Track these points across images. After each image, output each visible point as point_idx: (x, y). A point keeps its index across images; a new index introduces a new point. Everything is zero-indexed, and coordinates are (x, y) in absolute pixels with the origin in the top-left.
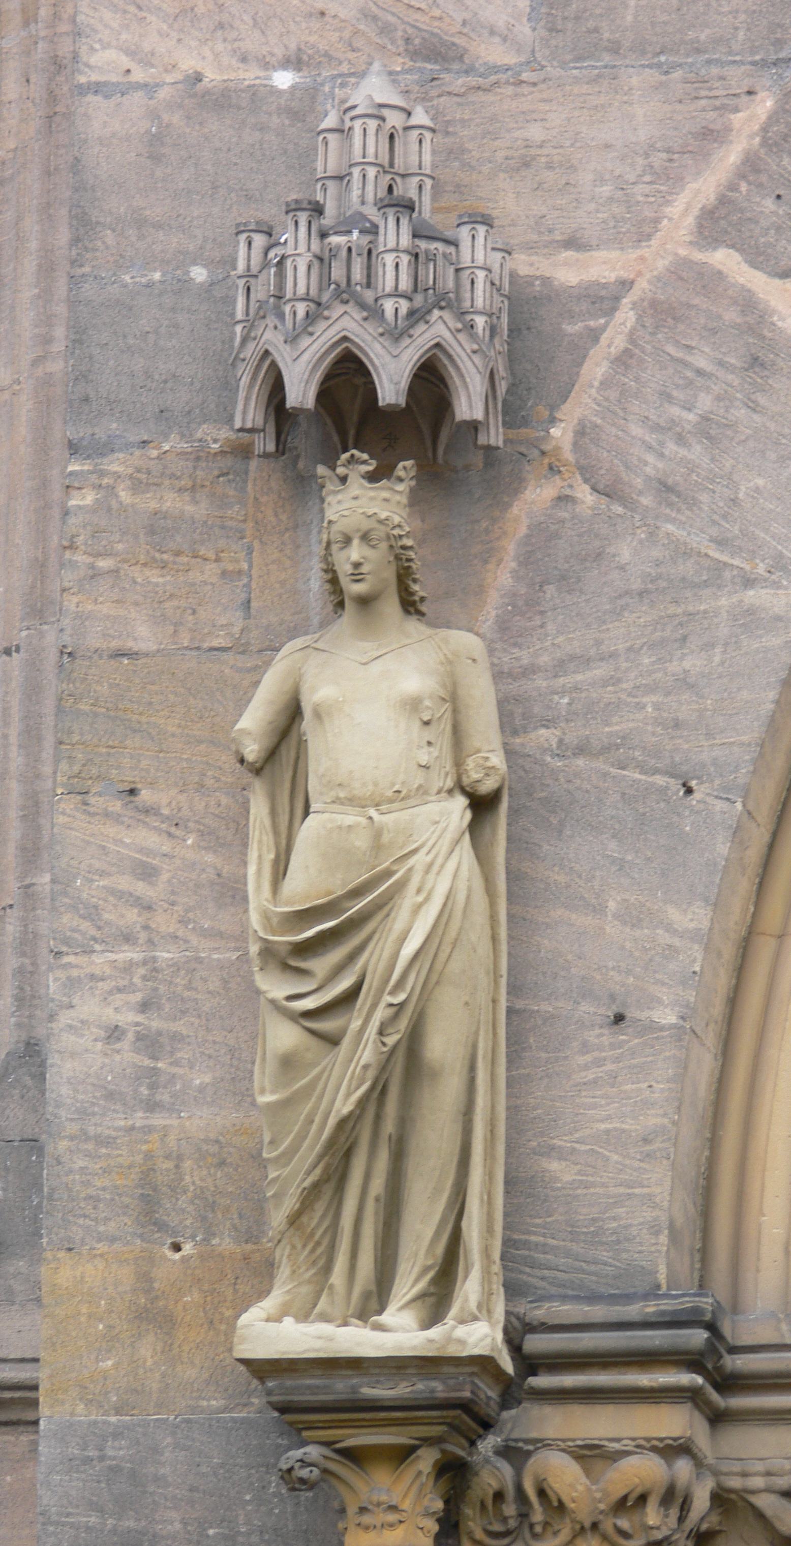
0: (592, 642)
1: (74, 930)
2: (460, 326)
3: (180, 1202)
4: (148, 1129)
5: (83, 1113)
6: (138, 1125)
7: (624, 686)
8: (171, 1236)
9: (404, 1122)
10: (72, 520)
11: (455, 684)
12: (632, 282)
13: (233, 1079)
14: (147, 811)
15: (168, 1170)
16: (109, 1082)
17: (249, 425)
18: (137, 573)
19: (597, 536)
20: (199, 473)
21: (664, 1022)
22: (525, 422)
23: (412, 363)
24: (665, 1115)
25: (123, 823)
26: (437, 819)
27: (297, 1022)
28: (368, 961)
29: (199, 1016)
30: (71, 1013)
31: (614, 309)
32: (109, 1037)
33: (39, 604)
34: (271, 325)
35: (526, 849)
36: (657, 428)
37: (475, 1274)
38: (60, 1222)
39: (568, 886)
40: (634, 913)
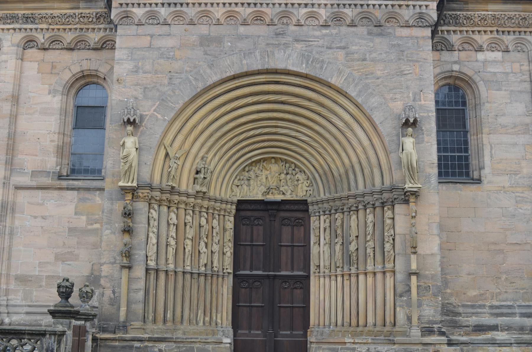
9: (131, 170)
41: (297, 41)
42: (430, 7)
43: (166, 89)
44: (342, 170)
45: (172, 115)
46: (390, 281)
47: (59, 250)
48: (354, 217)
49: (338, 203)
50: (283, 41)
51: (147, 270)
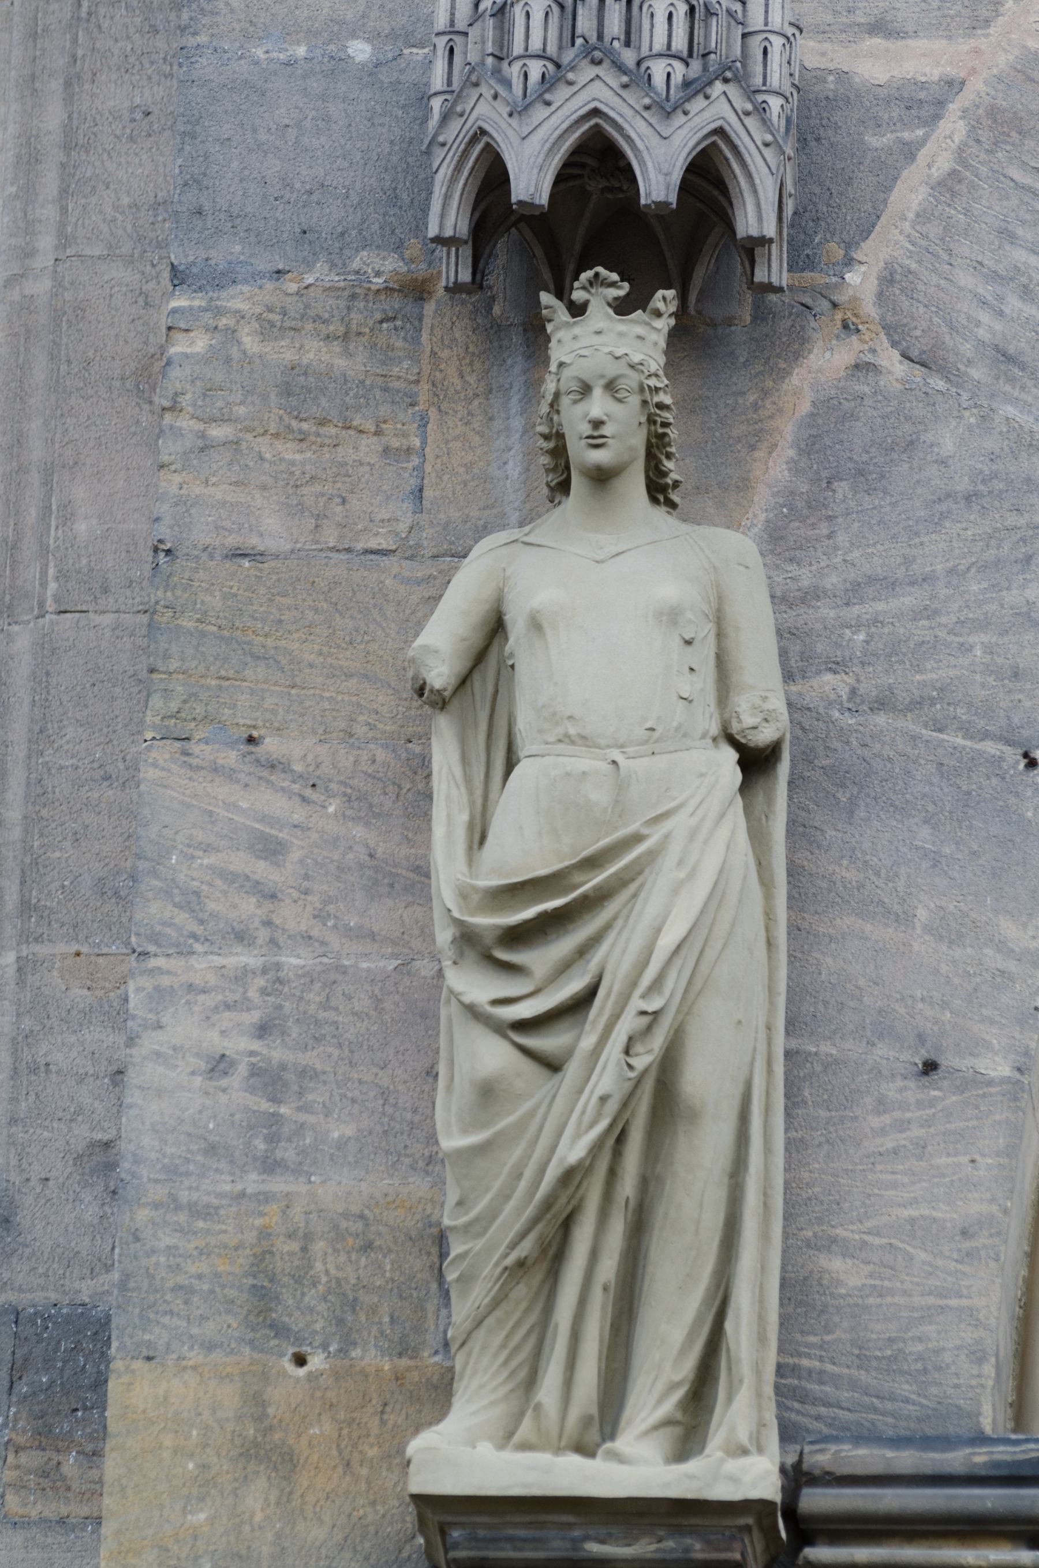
0: (899, 560)
1: (164, 924)
2: (749, 107)
3: (307, 1299)
4: (266, 1197)
5: (173, 1172)
6: (249, 1191)
7: (944, 620)
8: (293, 1344)
9: (647, 1184)
10: (175, 373)
11: (720, 599)
12: (963, 83)
13: (385, 1132)
14: (273, 766)
15: (291, 1254)
16: (210, 1132)
17: (448, 233)
18: (264, 446)
19: (908, 418)
20: (353, 315)
21: (993, 1074)
22: (810, 264)
23: (687, 150)
24: (993, 1200)
25: (238, 781)
26: (704, 770)
27: (505, 1037)
28: (608, 955)
29: (340, 1046)
30: (161, 1036)
31: (937, 117)
32: (212, 1070)
33: (7, 598)
34: (488, 94)
35: (804, 835)
36: (995, 277)
37: (744, 1397)
38: (137, 1321)
39: (861, 886)
40: (953, 924)
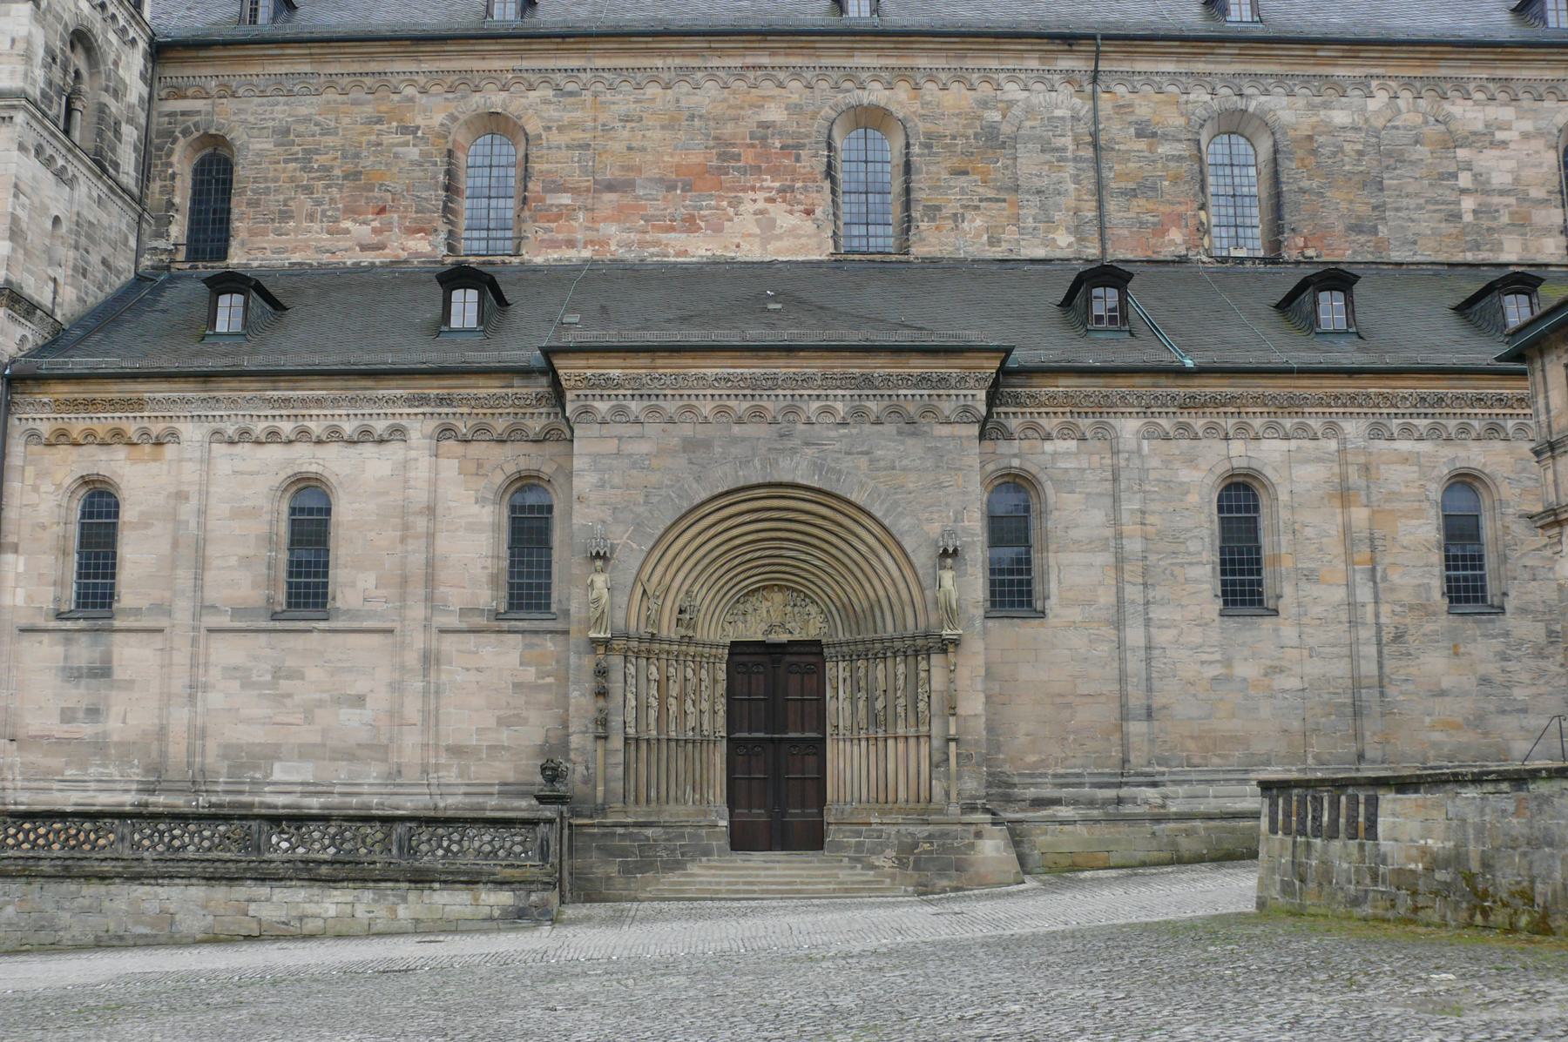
41: (807, 444)
42: (978, 397)
43: (641, 509)
44: (865, 604)
45: (651, 544)
46: (924, 749)
47: (502, 712)
48: (881, 666)
49: (860, 647)
50: (789, 444)
51: (626, 739)
